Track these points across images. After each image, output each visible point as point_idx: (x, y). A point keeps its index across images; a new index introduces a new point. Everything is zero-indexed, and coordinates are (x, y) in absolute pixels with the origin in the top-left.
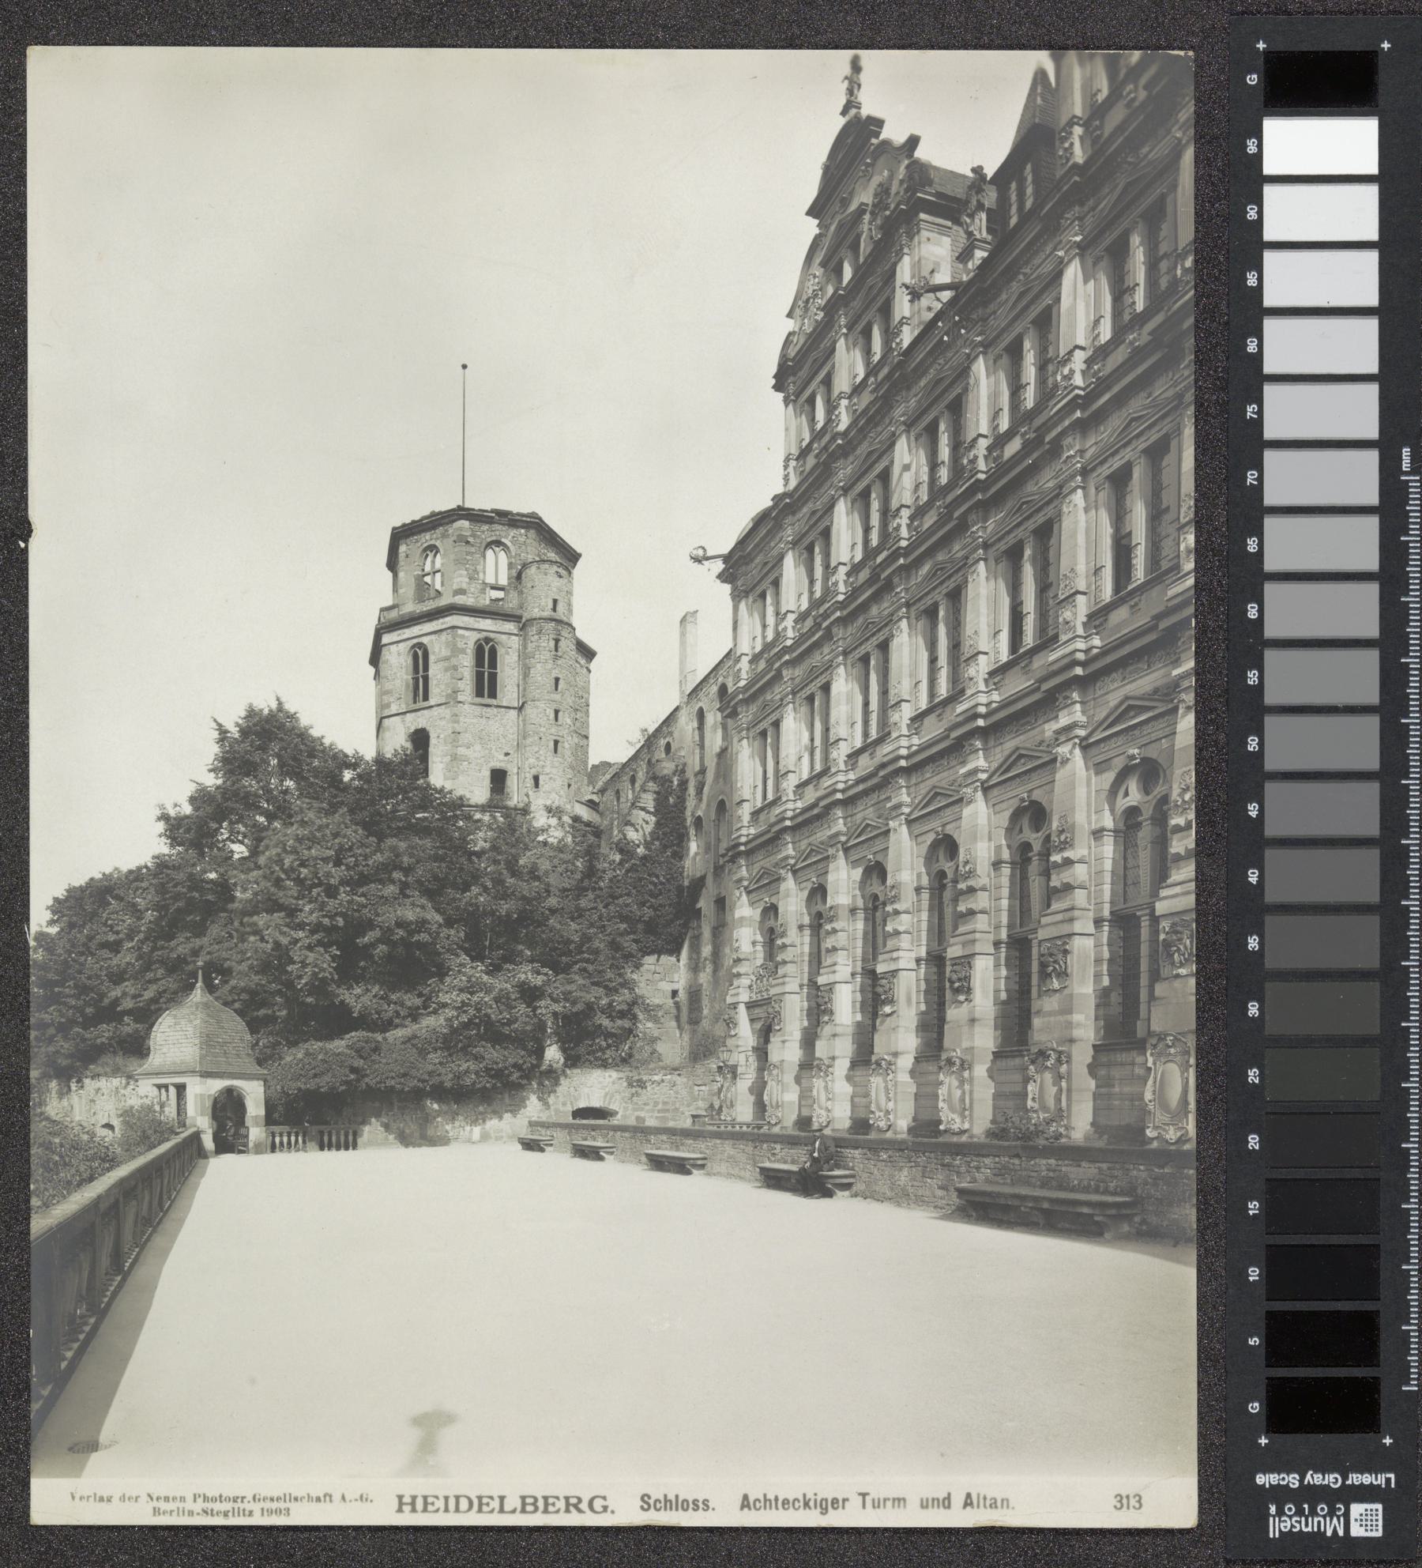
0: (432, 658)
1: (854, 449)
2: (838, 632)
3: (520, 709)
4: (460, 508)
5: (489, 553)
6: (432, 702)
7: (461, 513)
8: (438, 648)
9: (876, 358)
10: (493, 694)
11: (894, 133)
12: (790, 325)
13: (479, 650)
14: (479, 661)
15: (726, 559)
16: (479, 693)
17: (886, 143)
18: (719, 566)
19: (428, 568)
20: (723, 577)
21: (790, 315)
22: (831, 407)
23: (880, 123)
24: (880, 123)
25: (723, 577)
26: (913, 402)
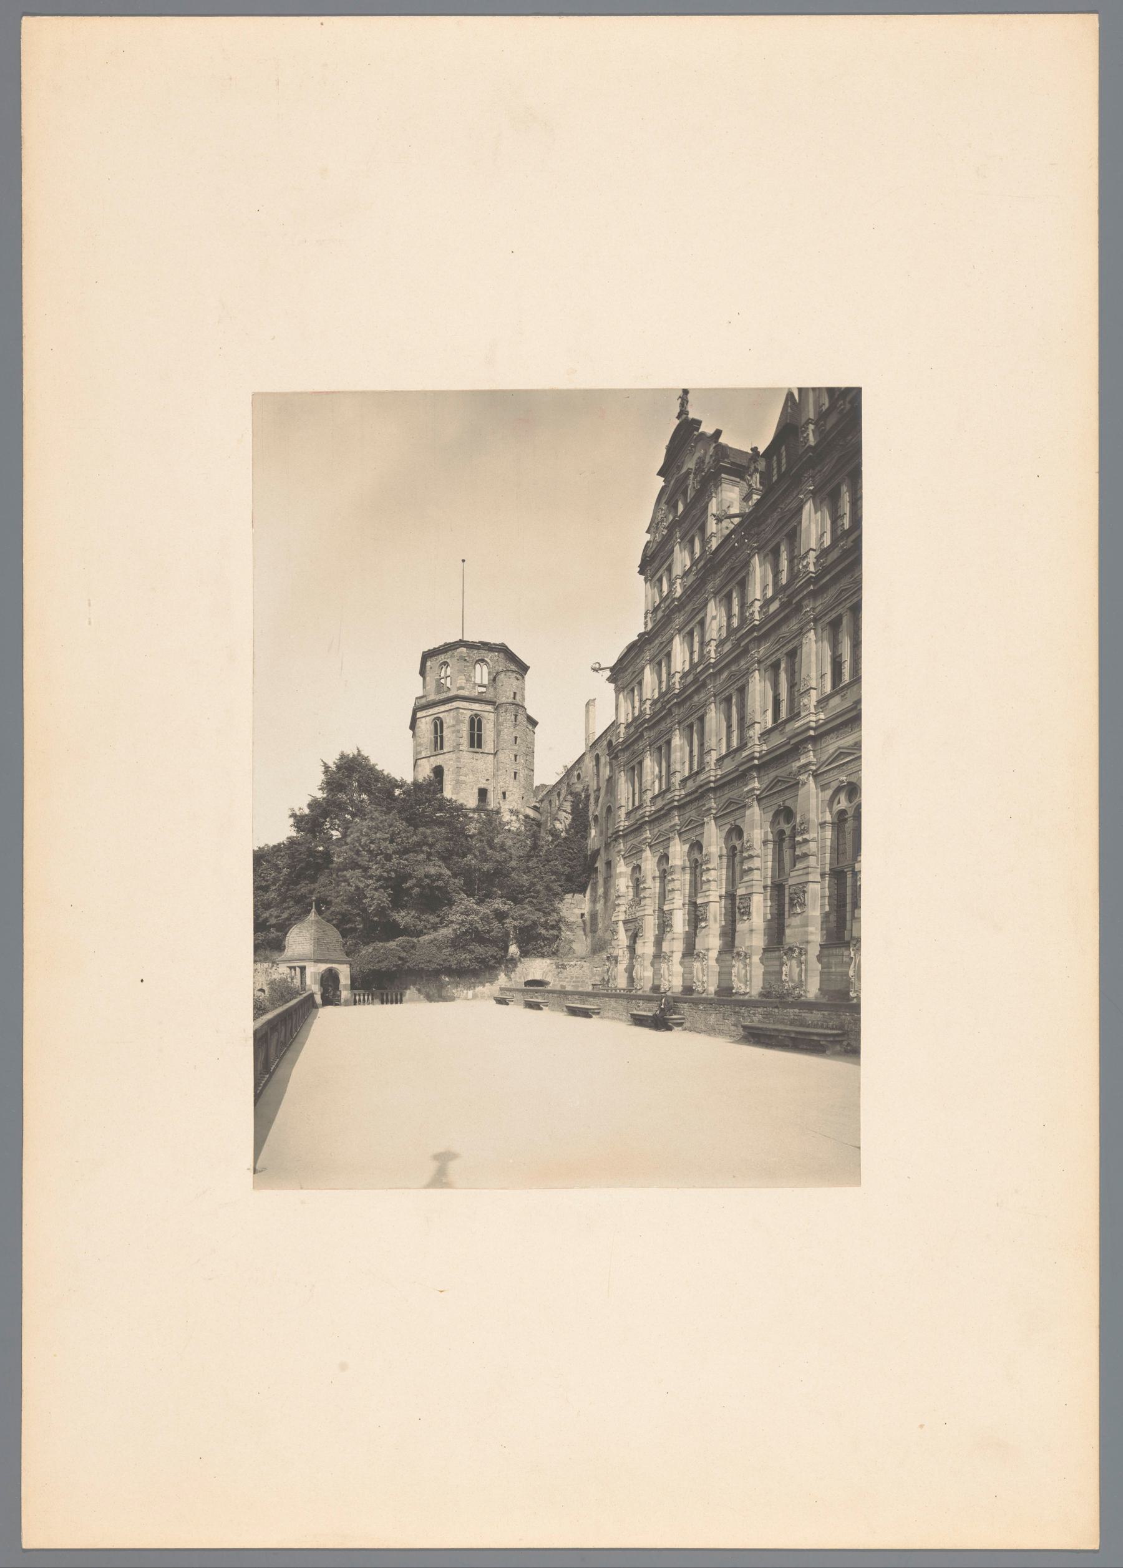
0: (445, 726)
1: (684, 607)
2: (675, 711)
3: (495, 754)
4: (461, 641)
5: (478, 666)
6: (445, 750)
7: (462, 643)
8: (448, 720)
9: (697, 556)
10: (480, 746)
11: (707, 428)
12: (648, 537)
13: (472, 721)
14: (472, 727)
15: (612, 669)
16: (472, 745)
17: (703, 434)
18: (608, 673)
19: (443, 675)
20: (610, 680)
21: (648, 532)
22: (671, 584)
23: (699, 423)
24: (699, 423)
25: (610, 680)
26: (718, 581)
